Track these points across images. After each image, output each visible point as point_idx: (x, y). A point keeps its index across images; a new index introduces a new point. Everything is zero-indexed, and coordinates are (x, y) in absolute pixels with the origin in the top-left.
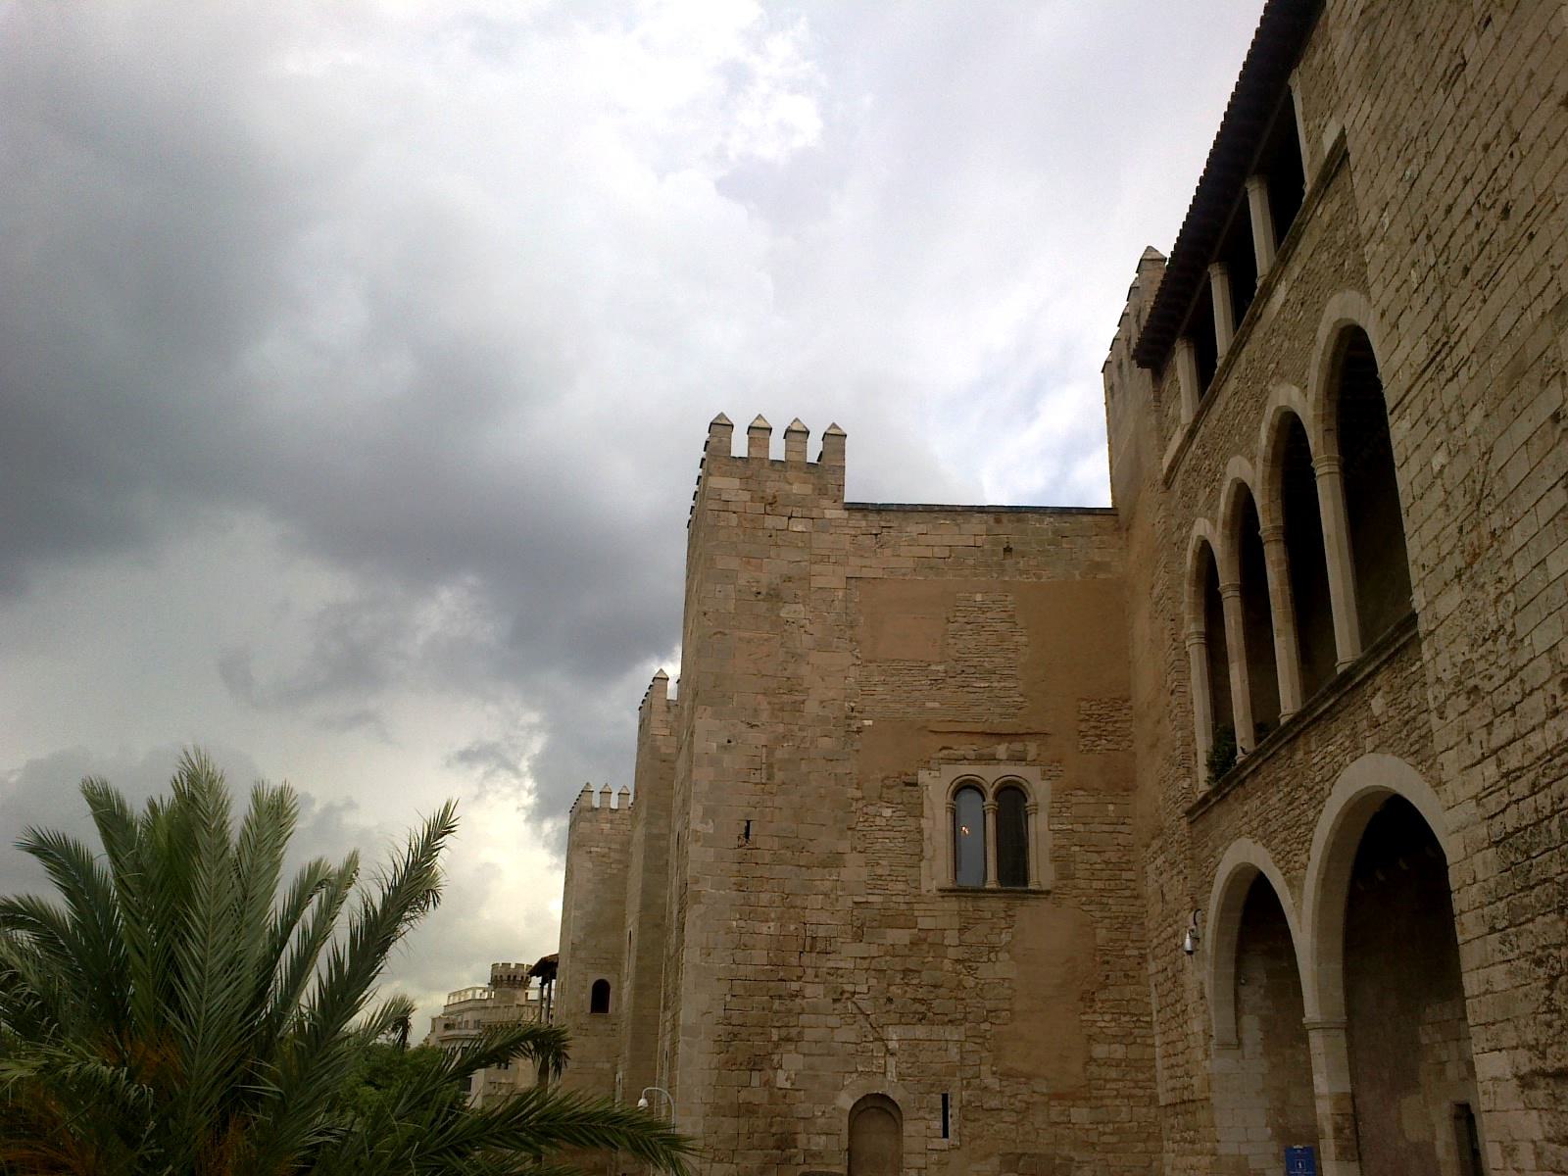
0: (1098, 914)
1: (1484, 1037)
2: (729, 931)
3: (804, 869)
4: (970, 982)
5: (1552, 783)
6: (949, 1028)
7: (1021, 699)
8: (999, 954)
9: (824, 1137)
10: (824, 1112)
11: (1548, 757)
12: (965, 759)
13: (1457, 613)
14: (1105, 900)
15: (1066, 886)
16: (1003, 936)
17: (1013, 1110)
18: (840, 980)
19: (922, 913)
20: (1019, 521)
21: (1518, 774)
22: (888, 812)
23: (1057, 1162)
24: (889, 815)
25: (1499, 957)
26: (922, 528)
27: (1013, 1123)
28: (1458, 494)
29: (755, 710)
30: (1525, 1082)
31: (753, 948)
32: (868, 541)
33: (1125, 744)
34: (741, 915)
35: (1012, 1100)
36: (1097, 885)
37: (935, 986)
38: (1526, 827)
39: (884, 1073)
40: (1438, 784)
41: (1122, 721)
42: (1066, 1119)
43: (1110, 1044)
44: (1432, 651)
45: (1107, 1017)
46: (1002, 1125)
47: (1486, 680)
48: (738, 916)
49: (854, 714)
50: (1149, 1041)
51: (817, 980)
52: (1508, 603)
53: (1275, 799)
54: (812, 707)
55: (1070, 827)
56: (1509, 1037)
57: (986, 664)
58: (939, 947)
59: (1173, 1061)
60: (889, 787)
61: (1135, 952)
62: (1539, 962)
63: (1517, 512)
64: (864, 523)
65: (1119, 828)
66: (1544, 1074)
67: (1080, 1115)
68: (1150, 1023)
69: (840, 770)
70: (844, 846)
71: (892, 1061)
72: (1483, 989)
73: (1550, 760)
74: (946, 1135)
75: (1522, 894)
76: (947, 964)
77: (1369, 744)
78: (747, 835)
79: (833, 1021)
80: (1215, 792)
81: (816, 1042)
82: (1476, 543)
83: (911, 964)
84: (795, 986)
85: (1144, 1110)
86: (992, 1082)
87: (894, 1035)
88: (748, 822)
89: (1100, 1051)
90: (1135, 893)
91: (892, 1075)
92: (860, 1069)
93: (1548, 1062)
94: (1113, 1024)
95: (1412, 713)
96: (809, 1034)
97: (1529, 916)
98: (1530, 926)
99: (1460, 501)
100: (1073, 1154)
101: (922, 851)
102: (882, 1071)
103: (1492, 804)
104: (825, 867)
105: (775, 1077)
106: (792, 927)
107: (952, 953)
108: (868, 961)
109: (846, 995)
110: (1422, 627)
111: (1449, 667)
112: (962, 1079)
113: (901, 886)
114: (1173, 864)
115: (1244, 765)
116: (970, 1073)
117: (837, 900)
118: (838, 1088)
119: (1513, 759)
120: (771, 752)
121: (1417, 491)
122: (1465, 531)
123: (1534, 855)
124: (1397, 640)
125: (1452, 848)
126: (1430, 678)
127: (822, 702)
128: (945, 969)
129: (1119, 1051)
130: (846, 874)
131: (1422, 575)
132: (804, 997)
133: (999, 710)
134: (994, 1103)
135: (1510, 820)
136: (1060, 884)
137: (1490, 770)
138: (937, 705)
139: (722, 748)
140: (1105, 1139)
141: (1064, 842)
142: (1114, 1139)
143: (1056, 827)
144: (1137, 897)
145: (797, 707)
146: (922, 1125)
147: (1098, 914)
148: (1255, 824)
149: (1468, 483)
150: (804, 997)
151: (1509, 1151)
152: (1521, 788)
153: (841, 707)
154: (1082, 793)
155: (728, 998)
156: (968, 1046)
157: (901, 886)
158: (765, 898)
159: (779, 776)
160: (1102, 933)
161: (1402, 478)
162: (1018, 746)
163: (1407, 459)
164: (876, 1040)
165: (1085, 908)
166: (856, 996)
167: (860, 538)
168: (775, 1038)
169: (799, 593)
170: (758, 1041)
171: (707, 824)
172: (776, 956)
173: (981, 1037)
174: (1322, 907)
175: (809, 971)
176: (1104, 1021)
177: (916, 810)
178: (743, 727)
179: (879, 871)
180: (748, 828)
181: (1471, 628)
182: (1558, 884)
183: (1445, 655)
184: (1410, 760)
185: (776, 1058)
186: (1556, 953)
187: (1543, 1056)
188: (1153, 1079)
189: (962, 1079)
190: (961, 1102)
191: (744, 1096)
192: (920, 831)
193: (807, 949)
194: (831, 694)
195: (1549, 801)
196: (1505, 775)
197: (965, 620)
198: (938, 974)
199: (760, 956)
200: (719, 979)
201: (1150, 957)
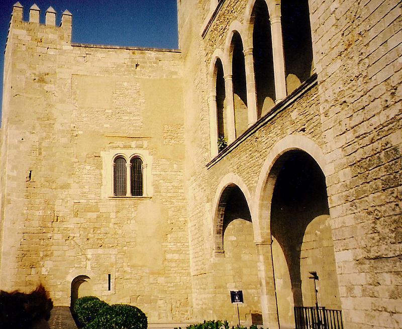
0: (169, 206)
1: (340, 245)
2: (23, 214)
3: (54, 190)
4: (120, 232)
5: (381, 138)
6: (111, 249)
7: (142, 124)
8: (131, 221)
9: (61, 292)
10: (61, 283)
11: (381, 127)
12: (119, 147)
13: (338, 71)
14: (172, 201)
15: (157, 195)
16: (133, 214)
17: (136, 279)
18: (68, 232)
19: (101, 206)
20: (142, 53)
21: (364, 136)
22: (88, 167)
23: (152, 297)
24: (89, 168)
25: (350, 212)
26: (103, 55)
27: (135, 284)
28: (343, 19)
29: (34, 126)
30: (359, 262)
31: (33, 220)
32: (81, 59)
33: (181, 142)
34: (28, 208)
35: (135, 275)
36: (169, 195)
37: (106, 233)
38: (367, 158)
39: (86, 267)
40: (322, 144)
41: (180, 133)
42: (155, 282)
43: (173, 254)
44: (324, 89)
45: (172, 244)
46: (132, 285)
47: (350, 98)
48: (26, 208)
49: (75, 129)
50: (188, 253)
51: (59, 232)
52: (364, 64)
53: (244, 157)
54: (57, 126)
55: (159, 173)
56: (352, 243)
57: (128, 110)
58: (108, 219)
59: (197, 259)
60: (89, 158)
61: (183, 219)
62: (369, 213)
63: (373, 22)
64: (79, 52)
65: (178, 173)
66: (369, 259)
67: (161, 280)
68: (188, 246)
69: (69, 152)
70: (70, 181)
71: (89, 263)
72: (340, 225)
73: (382, 128)
74: (109, 289)
75: (363, 186)
76: (111, 225)
77: (289, 132)
78: (30, 177)
79: (65, 248)
80: (219, 156)
81: (58, 256)
82: (350, 39)
83: (97, 225)
84: (49, 235)
85: (185, 277)
86: (128, 269)
87: (90, 253)
88: (31, 171)
89: (169, 256)
90: (184, 198)
91: (89, 268)
92: (76, 266)
93: (372, 254)
94: (174, 246)
95: (311, 117)
96: (55, 253)
97: (366, 195)
98: (366, 198)
99: (344, 23)
100: (158, 295)
101: (102, 183)
102: (85, 266)
103: (349, 150)
104: (63, 189)
105: (41, 270)
106: (49, 212)
107: (113, 221)
108: (79, 224)
109: (70, 238)
110: (319, 79)
111: (331, 94)
112: (116, 268)
113: (93, 196)
114: (200, 185)
115: (231, 146)
116: (119, 265)
117: (67, 202)
118: (67, 273)
119: (361, 130)
120: (40, 144)
121: (322, 21)
122: (345, 35)
123: (370, 169)
124: (306, 86)
125: (328, 170)
126: (322, 100)
127: (61, 124)
128: (110, 227)
129: (176, 256)
130: (71, 191)
131: (322, 57)
132: (53, 239)
133: (133, 128)
134: (128, 277)
135: (358, 156)
136: (155, 194)
137: (350, 136)
138: (108, 126)
139: (19, 141)
140: (170, 289)
141: (157, 178)
142: (174, 289)
143: (155, 173)
144: (184, 199)
145: (51, 126)
146: (100, 286)
147: (169, 206)
148: (235, 167)
149: (349, 13)
150: (53, 239)
151: (350, 289)
152: (367, 140)
153: (70, 126)
154: (164, 160)
155: (22, 240)
156: (119, 256)
157: (93, 196)
158: (38, 201)
159: (44, 153)
160: (170, 213)
161: (313, 19)
162: (140, 142)
163: (318, 8)
164: (83, 254)
165: (165, 203)
166: (75, 238)
167: (78, 58)
168: (41, 255)
169: (52, 80)
170: (34, 257)
171: (13, 172)
172: (42, 223)
173: (123, 252)
174: (263, 199)
175: (56, 229)
176: (171, 246)
177: (99, 166)
178: (28, 134)
179: (84, 190)
180: (30, 174)
181: (345, 77)
182: (382, 180)
183: (330, 90)
184: (310, 136)
185: (42, 263)
186: (378, 208)
187: (369, 251)
188: (189, 266)
189: (116, 268)
190: (116, 276)
191: (28, 278)
192: (101, 175)
193: (55, 220)
194: (66, 121)
195: (380, 145)
196: (357, 137)
197: (120, 93)
198: (107, 229)
199: (36, 224)
200: (18, 233)
201: (189, 221)
